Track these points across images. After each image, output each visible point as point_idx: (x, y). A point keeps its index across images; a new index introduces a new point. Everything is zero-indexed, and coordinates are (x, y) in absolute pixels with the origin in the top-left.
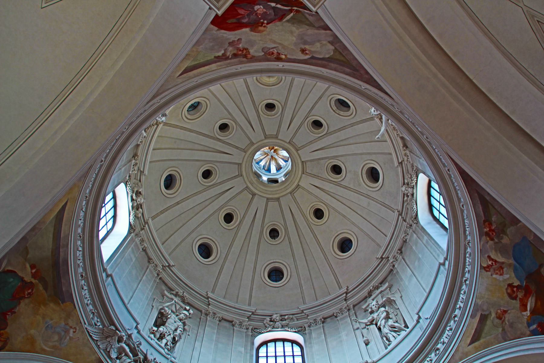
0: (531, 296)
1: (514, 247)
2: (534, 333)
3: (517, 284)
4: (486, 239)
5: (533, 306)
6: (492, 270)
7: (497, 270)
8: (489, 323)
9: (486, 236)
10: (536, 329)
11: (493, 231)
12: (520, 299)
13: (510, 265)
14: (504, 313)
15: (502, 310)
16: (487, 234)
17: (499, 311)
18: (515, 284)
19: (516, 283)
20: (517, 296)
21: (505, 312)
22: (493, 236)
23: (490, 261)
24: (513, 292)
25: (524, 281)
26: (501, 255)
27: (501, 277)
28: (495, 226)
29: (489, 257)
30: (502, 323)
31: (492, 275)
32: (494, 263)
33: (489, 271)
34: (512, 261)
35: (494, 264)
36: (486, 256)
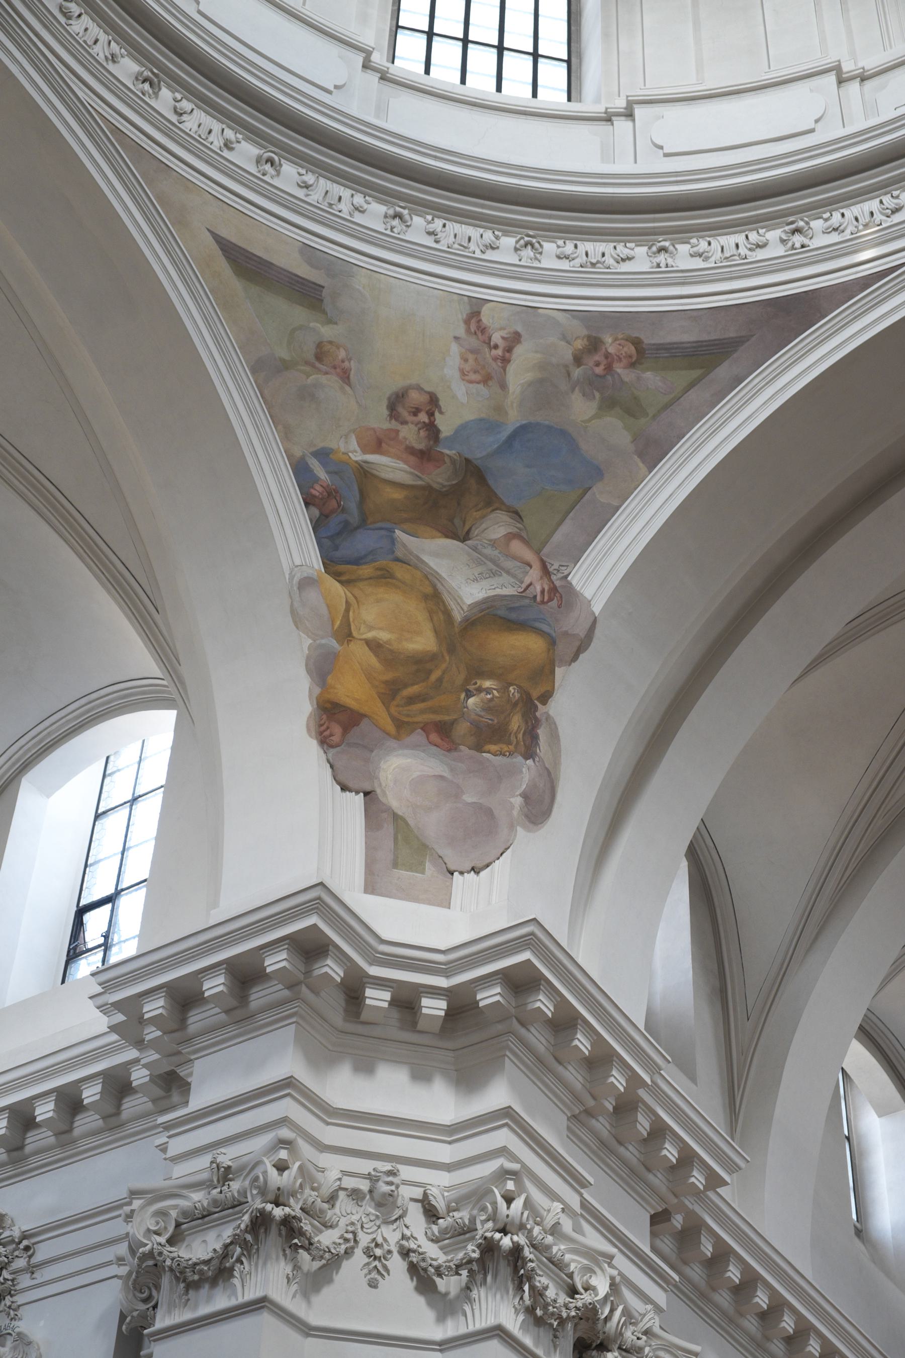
0: (412, 470)
1: (563, 433)
2: (301, 470)
3: (442, 427)
4: (577, 338)
5: (384, 475)
6: (474, 342)
7: (476, 359)
8: (298, 314)
9: (589, 337)
10: (317, 480)
11: (609, 368)
12: (397, 432)
13: (499, 409)
14: (338, 370)
15: (346, 364)
16: (594, 344)
17: (342, 354)
18: (439, 420)
19: (446, 425)
20: (404, 423)
21: (345, 377)
22: (591, 364)
23: (503, 338)
24: (416, 412)
25: (454, 452)
26: (530, 384)
27: (457, 374)
28: (626, 379)
29: (515, 339)
30: (307, 363)
31: (456, 338)
32: (499, 352)
33: (468, 331)
34: (514, 418)
35: (494, 352)
36: (519, 329)
